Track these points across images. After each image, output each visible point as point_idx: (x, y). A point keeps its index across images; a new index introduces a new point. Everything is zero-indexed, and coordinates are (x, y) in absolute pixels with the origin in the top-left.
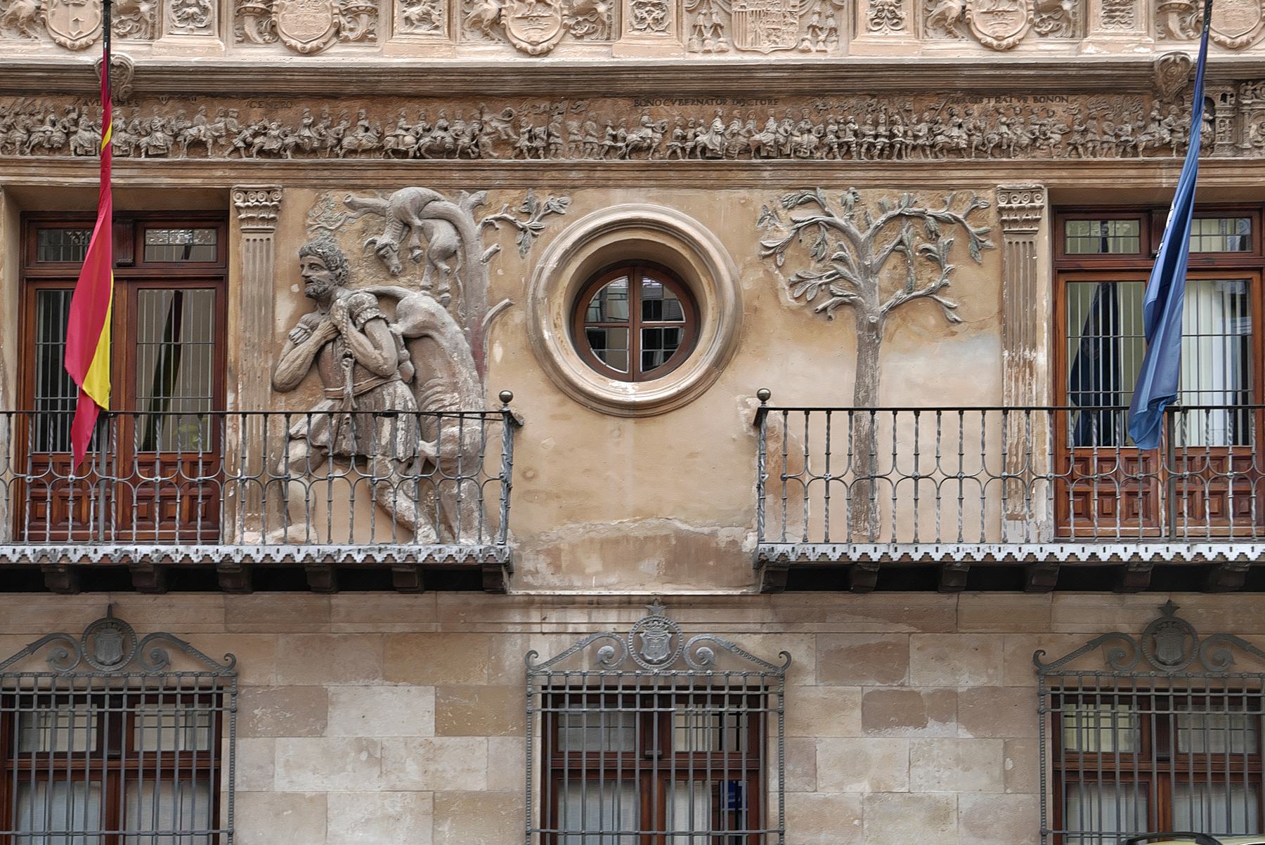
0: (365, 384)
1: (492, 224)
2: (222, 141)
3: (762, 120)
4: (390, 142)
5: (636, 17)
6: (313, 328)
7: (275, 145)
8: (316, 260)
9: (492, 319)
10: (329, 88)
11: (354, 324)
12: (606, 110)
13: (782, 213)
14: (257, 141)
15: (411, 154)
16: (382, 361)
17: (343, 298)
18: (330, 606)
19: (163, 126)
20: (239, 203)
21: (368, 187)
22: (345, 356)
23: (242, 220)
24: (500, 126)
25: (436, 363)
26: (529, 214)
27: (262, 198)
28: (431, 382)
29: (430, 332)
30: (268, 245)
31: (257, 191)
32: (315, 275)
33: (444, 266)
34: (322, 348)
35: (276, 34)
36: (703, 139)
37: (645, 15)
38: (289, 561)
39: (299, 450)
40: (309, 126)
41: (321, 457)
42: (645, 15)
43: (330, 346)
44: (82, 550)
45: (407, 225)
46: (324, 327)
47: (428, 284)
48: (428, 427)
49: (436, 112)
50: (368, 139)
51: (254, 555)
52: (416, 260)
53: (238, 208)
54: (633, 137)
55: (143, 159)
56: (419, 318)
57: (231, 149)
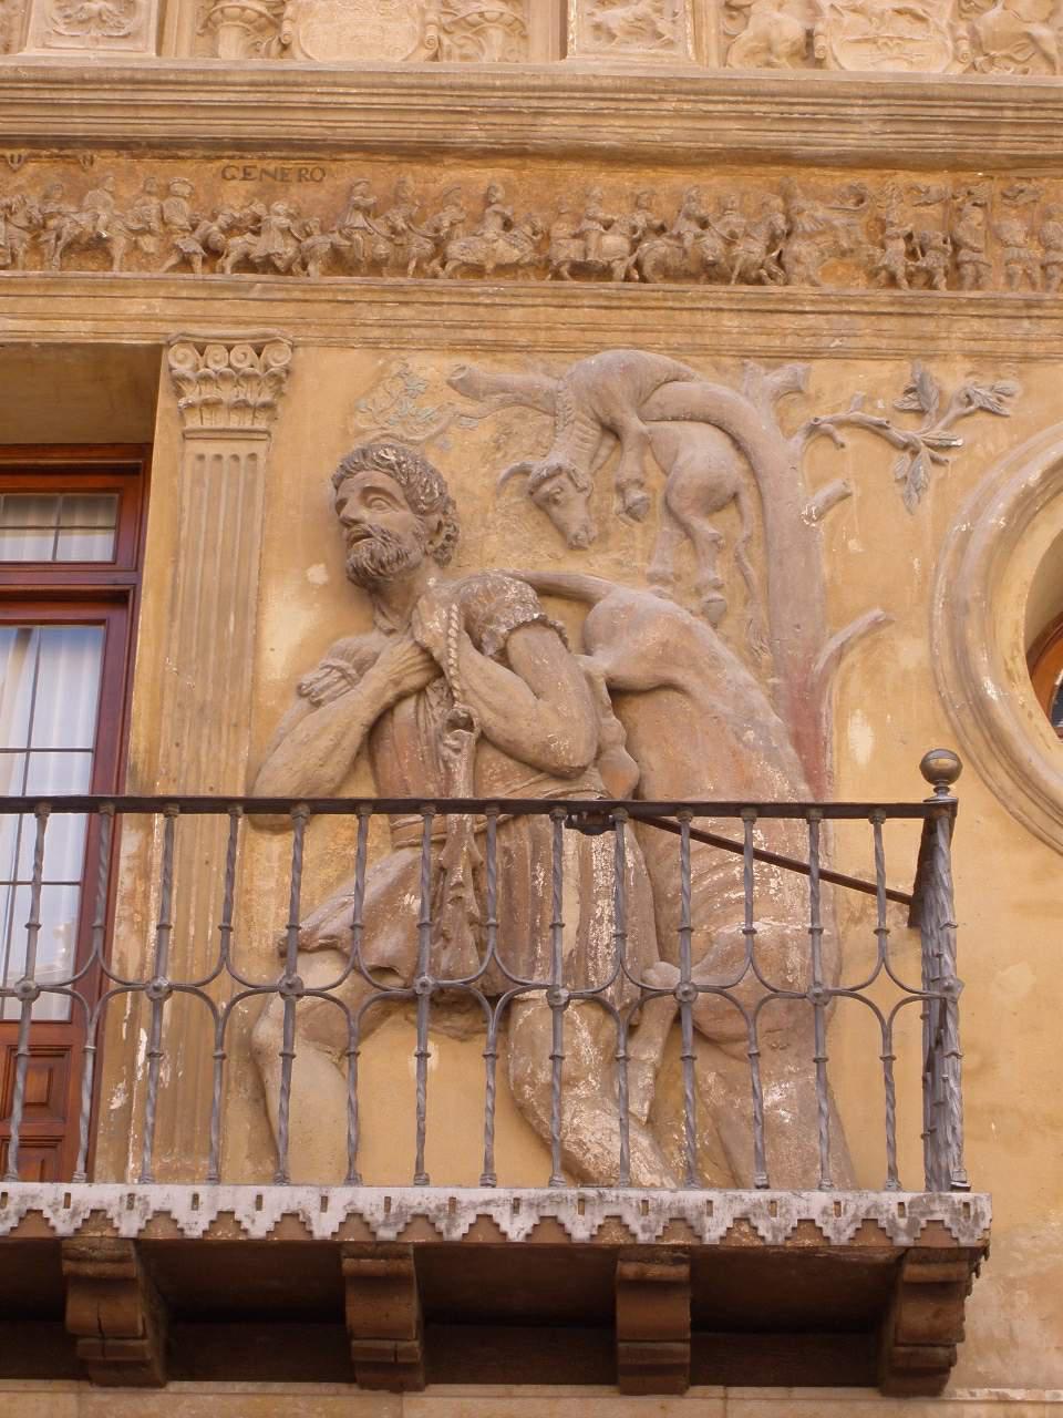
6: (362, 667)
8: (380, 479)
9: (839, 656)
10: (416, 129)
11: (479, 646)
14: (237, 240)
20: (183, 369)
22: (453, 724)
29: (679, 676)
32: (368, 516)
33: (705, 527)
34: (387, 712)
38: (292, 1234)
40: (367, 211)
43: (408, 707)
45: (612, 431)
46: (393, 659)
51: (182, 1213)
52: (631, 512)
56: (651, 637)
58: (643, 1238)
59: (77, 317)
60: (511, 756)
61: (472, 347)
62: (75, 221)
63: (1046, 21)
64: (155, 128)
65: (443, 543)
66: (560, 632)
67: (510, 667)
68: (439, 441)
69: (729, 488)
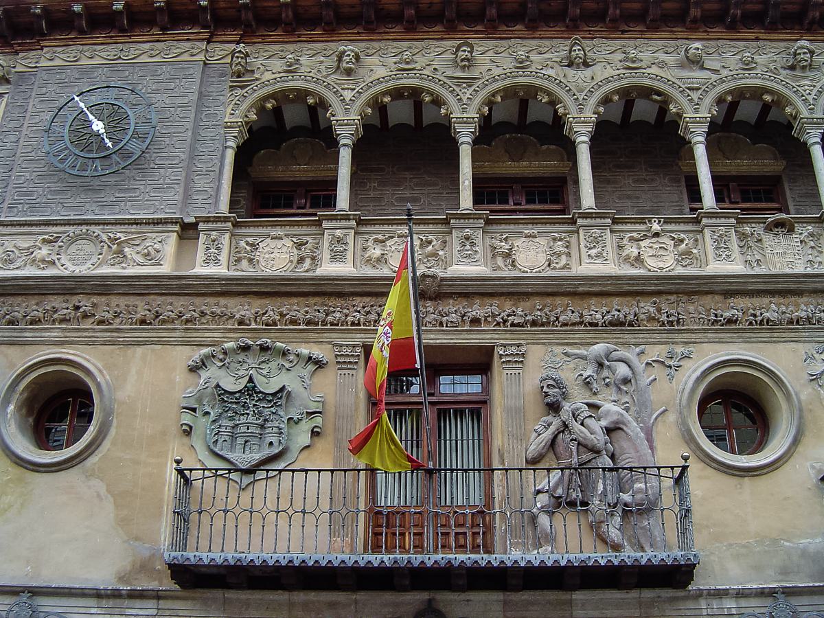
0: (586, 456)
1: (651, 364)
2: (489, 319)
3: (797, 306)
4: (587, 319)
5: (716, 254)
6: (549, 425)
7: (521, 320)
8: (551, 382)
9: (656, 419)
11: (576, 421)
12: (707, 300)
13: (817, 356)
15: (600, 324)
16: (596, 442)
17: (567, 407)
18: (571, 600)
19: (456, 311)
20: (501, 352)
21: (575, 344)
22: (571, 440)
23: (504, 362)
24: (652, 310)
25: (625, 444)
26: (672, 358)
27: (514, 350)
28: (624, 456)
30: (520, 376)
31: (511, 345)
32: (551, 391)
34: (555, 437)
35: (514, 266)
36: (767, 315)
37: (721, 253)
39: (543, 499)
40: (540, 310)
41: (559, 504)
42: (721, 253)
44: (420, 557)
45: (601, 365)
46: (556, 423)
47: (616, 399)
48: (624, 484)
49: (611, 302)
50: (575, 318)
52: (607, 385)
53: (501, 355)
54: (727, 314)
55: (444, 328)
56: (615, 418)
57: (495, 323)
58: (629, 564)
59: (475, 339)
60: (586, 448)
61: (567, 344)
62: (472, 314)
63: (695, 248)
64: (490, 290)
65: (565, 396)
66: (594, 417)
67: (584, 426)
68: (561, 368)
69: (629, 378)
